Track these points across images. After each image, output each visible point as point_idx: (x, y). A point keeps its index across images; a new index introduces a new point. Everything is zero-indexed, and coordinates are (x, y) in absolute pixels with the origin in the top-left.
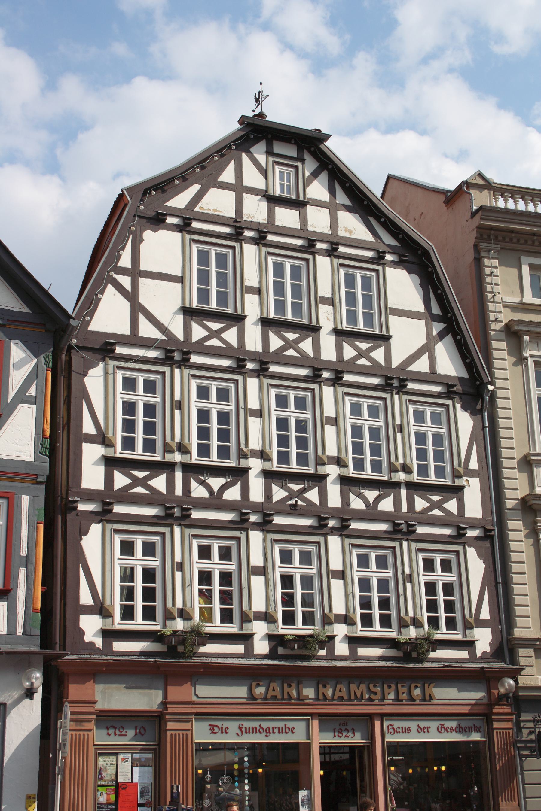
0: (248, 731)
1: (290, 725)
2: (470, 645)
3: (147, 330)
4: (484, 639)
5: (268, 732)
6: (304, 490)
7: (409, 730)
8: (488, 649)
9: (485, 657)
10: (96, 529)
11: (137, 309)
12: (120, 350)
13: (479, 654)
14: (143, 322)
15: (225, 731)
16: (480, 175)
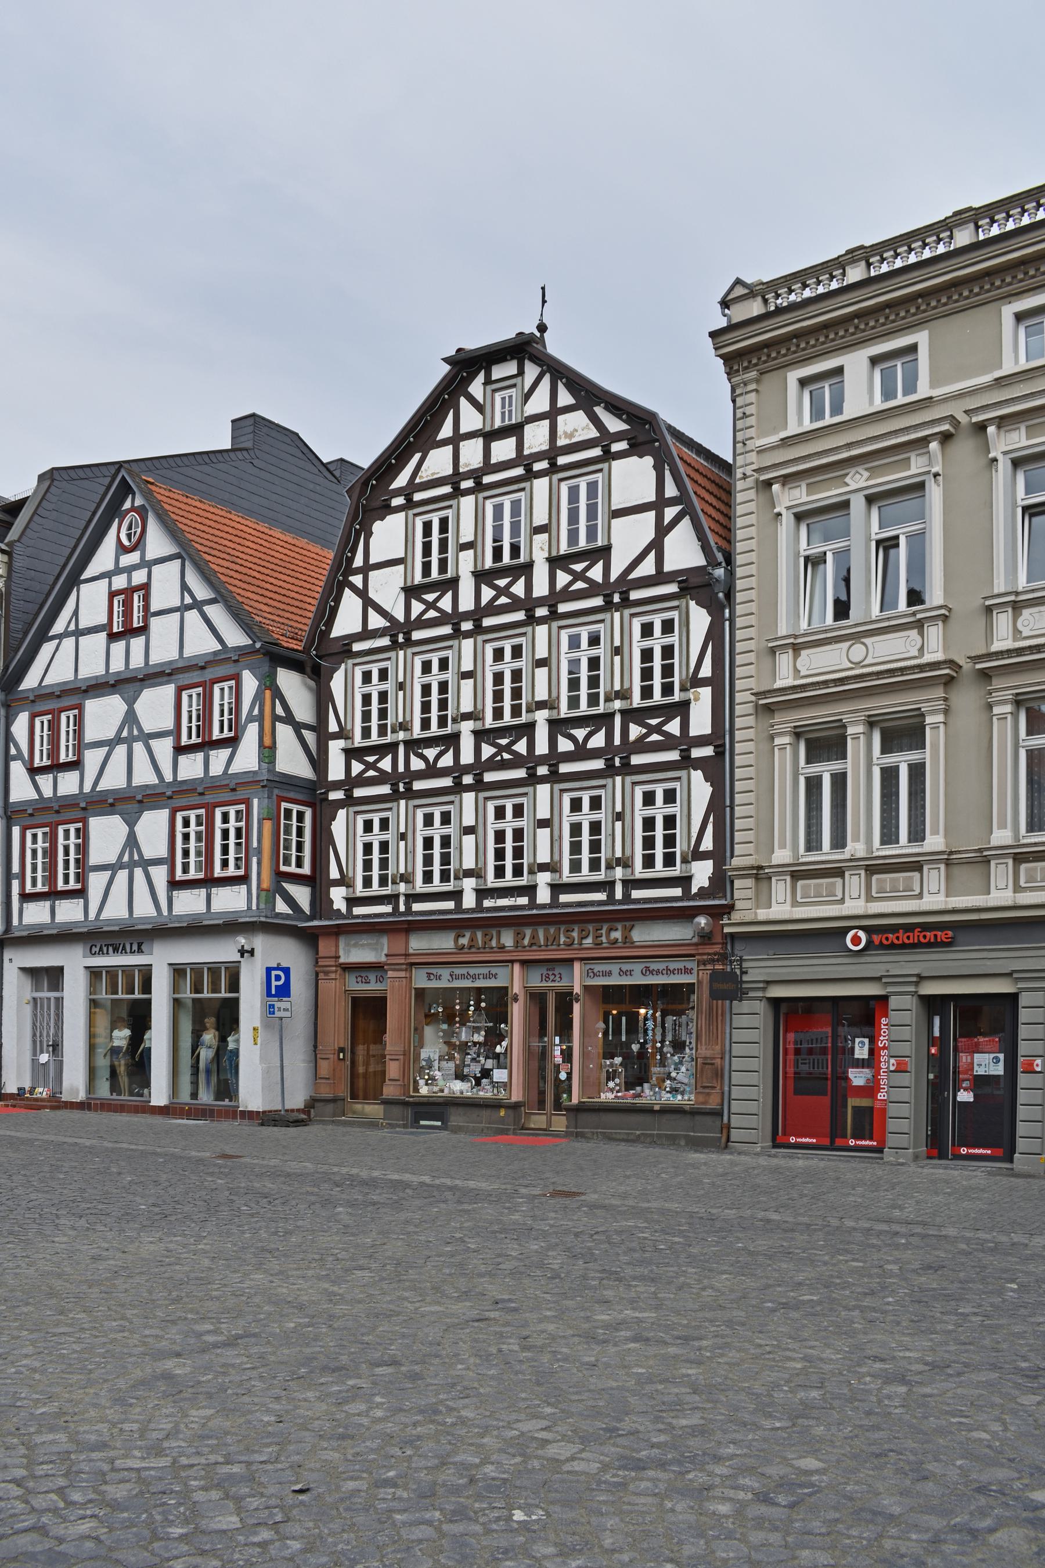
0: (458, 977)
1: (494, 971)
2: (685, 881)
3: (376, 621)
4: (702, 873)
5: (474, 978)
6: (513, 743)
7: (610, 973)
8: (706, 884)
9: (702, 893)
10: (342, 814)
11: (368, 603)
12: (357, 647)
13: (694, 890)
15: (439, 978)
16: (738, 282)
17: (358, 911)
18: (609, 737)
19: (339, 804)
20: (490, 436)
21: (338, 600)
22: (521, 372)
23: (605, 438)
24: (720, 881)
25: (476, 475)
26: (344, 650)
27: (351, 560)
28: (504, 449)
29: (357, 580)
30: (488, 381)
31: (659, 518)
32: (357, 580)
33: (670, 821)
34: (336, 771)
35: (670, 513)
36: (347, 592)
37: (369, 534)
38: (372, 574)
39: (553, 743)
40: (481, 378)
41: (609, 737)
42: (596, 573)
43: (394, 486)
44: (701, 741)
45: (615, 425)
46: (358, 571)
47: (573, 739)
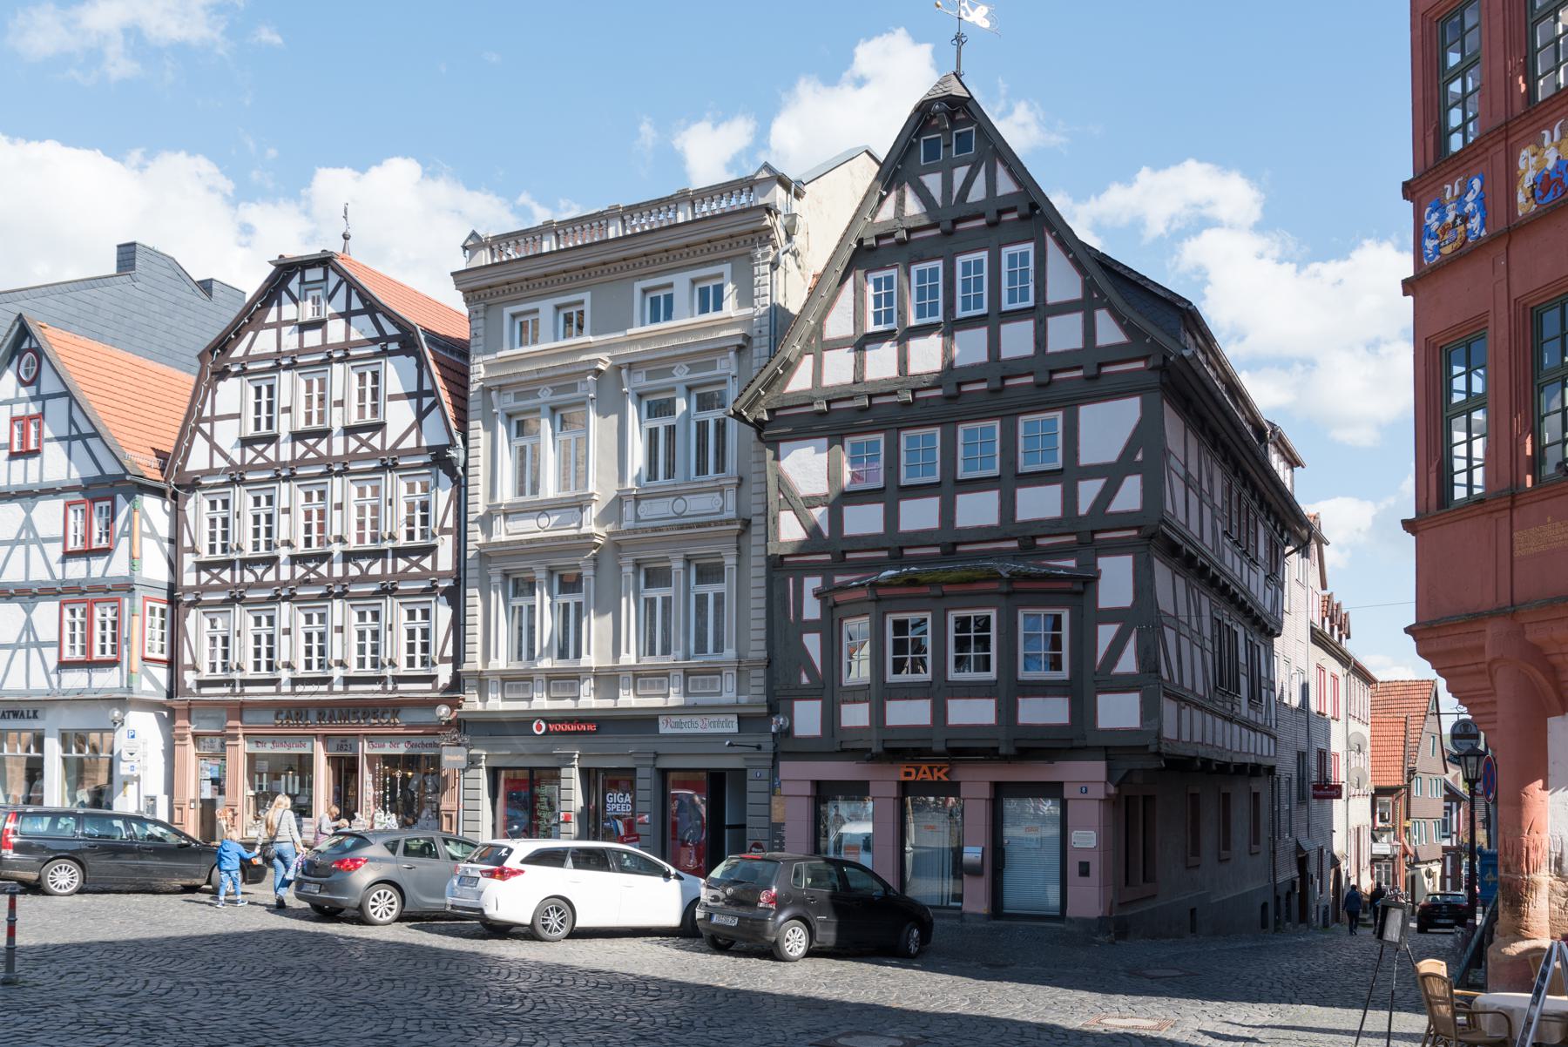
3: (220, 463)
4: (444, 673)
11: (214, 447)
14: (217, 458)
17: (205, 691)
18: (384, 566)
19: (192, 604)
20: (304, 327)
21: (191, 442)
22: (326, 278)
23: (383, 337)
24: (457, 683)
25: (293, 354)
26: (192, 485)
27: (201, 411)
28: (313, 338)
29: (206, 427)
30: (302, 282)
31: (419, 405)
32: (206, 427)
33: (425, 633)
34: (189, 579)
35: (427, 402)
36: (198, 435)
37: (215, 392)
38: (217, 424)
39: (346, 571)
40: (297, 278)
41: (384, 566)
42: (376, 442)
43: (234, 355)
44: (444, 575)
45: (391, 330)
46: (206, 420)
47: (360, 567)
